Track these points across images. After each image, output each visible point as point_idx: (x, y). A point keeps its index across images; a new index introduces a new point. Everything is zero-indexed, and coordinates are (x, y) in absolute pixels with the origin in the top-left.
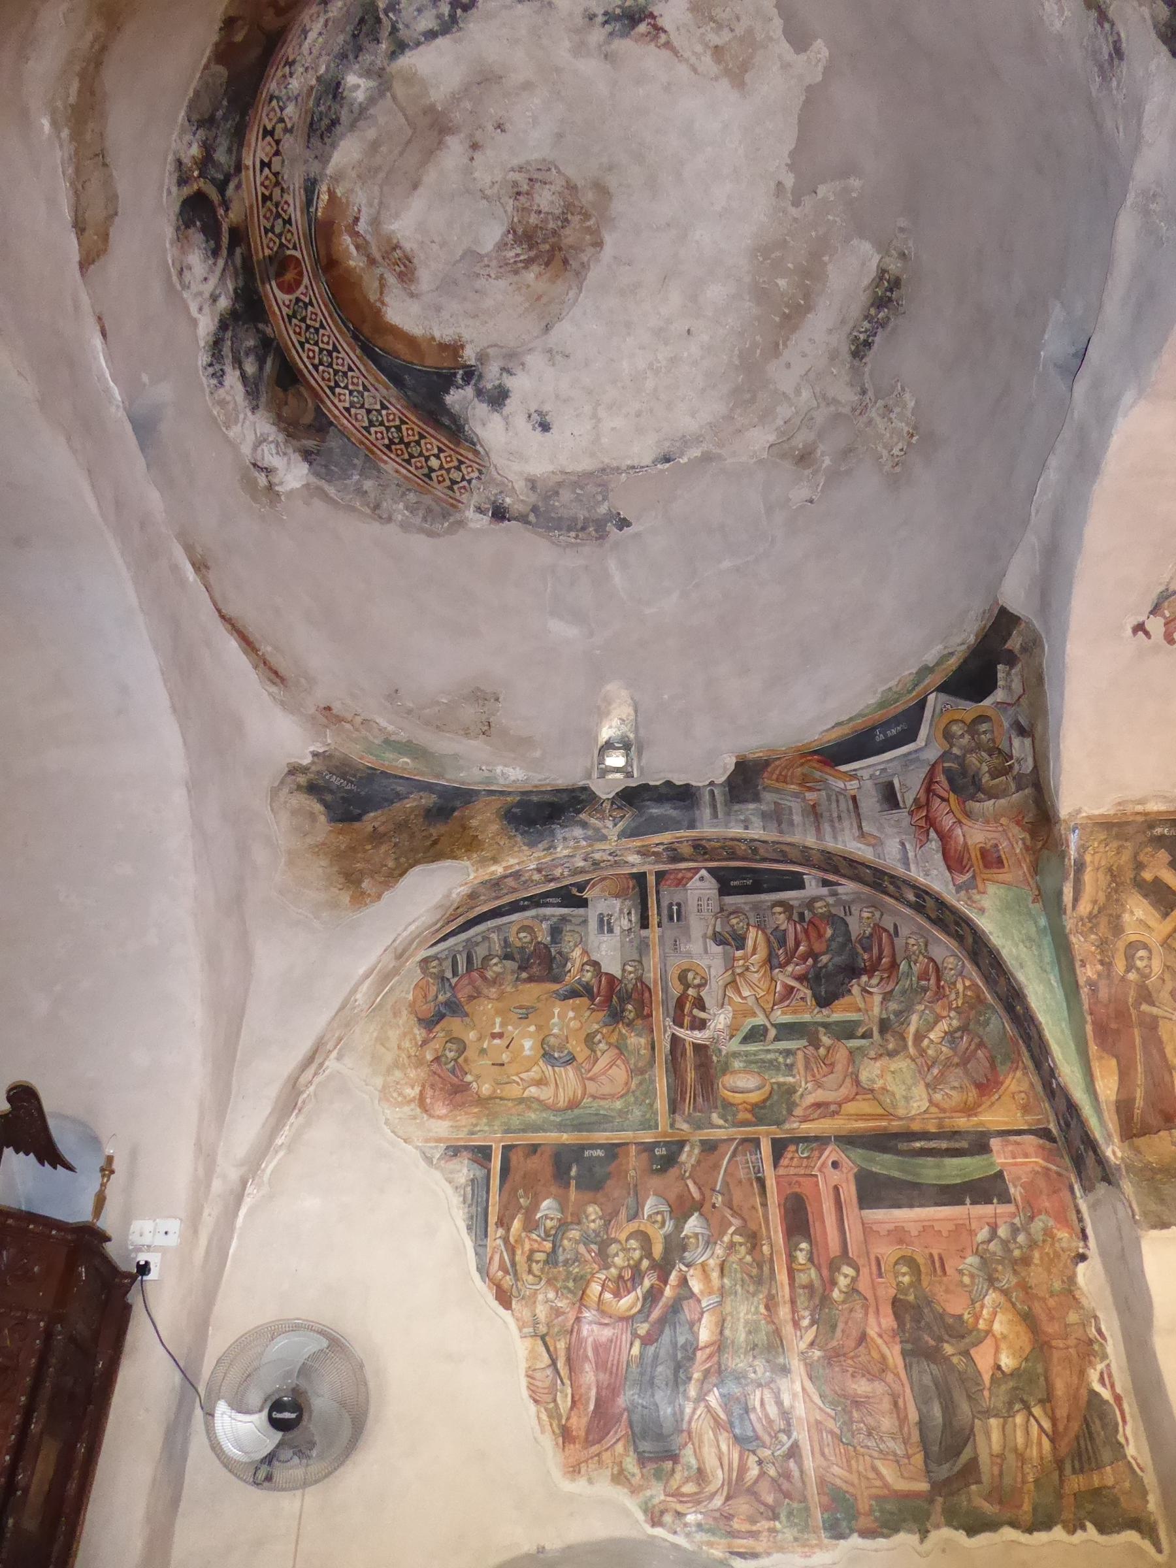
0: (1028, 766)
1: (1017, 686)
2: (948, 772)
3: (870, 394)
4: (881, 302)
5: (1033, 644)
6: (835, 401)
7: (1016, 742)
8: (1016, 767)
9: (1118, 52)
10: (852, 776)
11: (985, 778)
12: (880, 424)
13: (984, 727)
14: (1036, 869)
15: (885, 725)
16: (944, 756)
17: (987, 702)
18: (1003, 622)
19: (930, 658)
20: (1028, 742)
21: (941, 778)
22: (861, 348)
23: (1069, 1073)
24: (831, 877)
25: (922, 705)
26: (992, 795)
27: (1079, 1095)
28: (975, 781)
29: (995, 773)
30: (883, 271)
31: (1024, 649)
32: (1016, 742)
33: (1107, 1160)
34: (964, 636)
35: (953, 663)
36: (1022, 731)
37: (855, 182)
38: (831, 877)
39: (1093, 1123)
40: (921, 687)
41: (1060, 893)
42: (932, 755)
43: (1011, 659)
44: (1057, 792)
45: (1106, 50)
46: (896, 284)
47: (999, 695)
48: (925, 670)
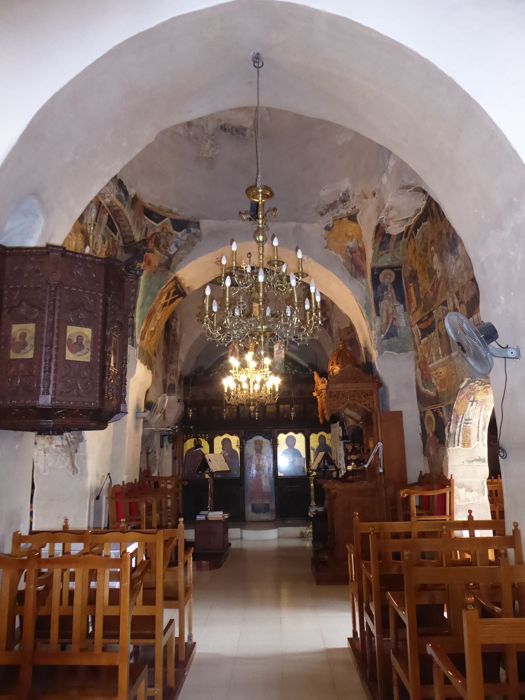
0: (172, 253)
1: (185, 237)
2: (156, 237)
3: (213, 137)
4: (237, 130)
5: (198, 236)
6: (207, 126)
7: (173, 246)
8: (168, 250)
9: (322, 215)
10: (145, 220)
11: (161, 246)
12: (208, 145)
13: (170, 235)
14: (154, 272)
15: (157, 214)
16: (159, 233)
17: (176, 232)
18: (197, 225)
19: (175, 210)
20: (176, 249)
21: (155, 237)
22: (224, 128)
23: (137, 320)
24: (121, 238)
25: (165, 218)
26: (159, 250)
27: (137, 326)
28: (160, 243)
29: (163, 246)
30: (245, 129)
31: (195, 234)
32: (173, 246)
33: (136, 342)
34: (183, 214)
35: (178, 217)
36: (176, 246)
37: (268, 119)
38: (121, 238)
39: (137, 333)
40: (168, 214)
41: (163, 286)
42: (158, 230)
43: (189, 232)
44: (179, 269)
45: (321, 210)
46: (244, 135)
47: (179, 234)
48: (170, 211)
